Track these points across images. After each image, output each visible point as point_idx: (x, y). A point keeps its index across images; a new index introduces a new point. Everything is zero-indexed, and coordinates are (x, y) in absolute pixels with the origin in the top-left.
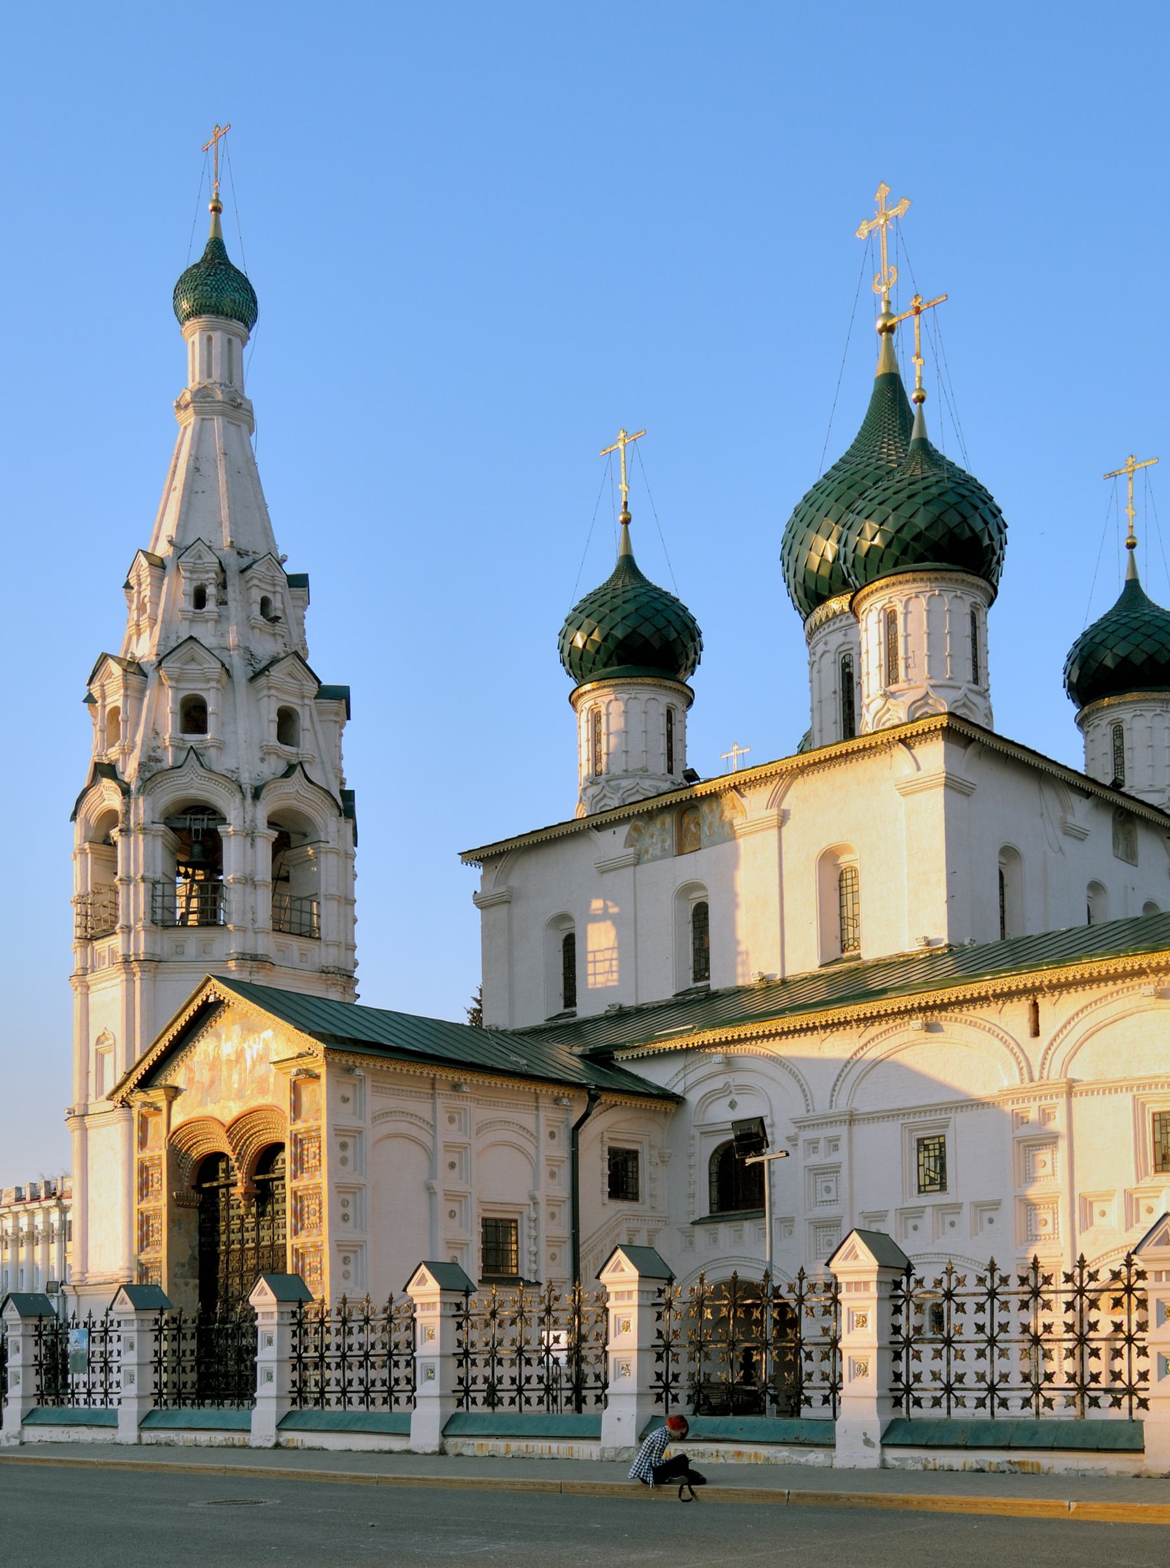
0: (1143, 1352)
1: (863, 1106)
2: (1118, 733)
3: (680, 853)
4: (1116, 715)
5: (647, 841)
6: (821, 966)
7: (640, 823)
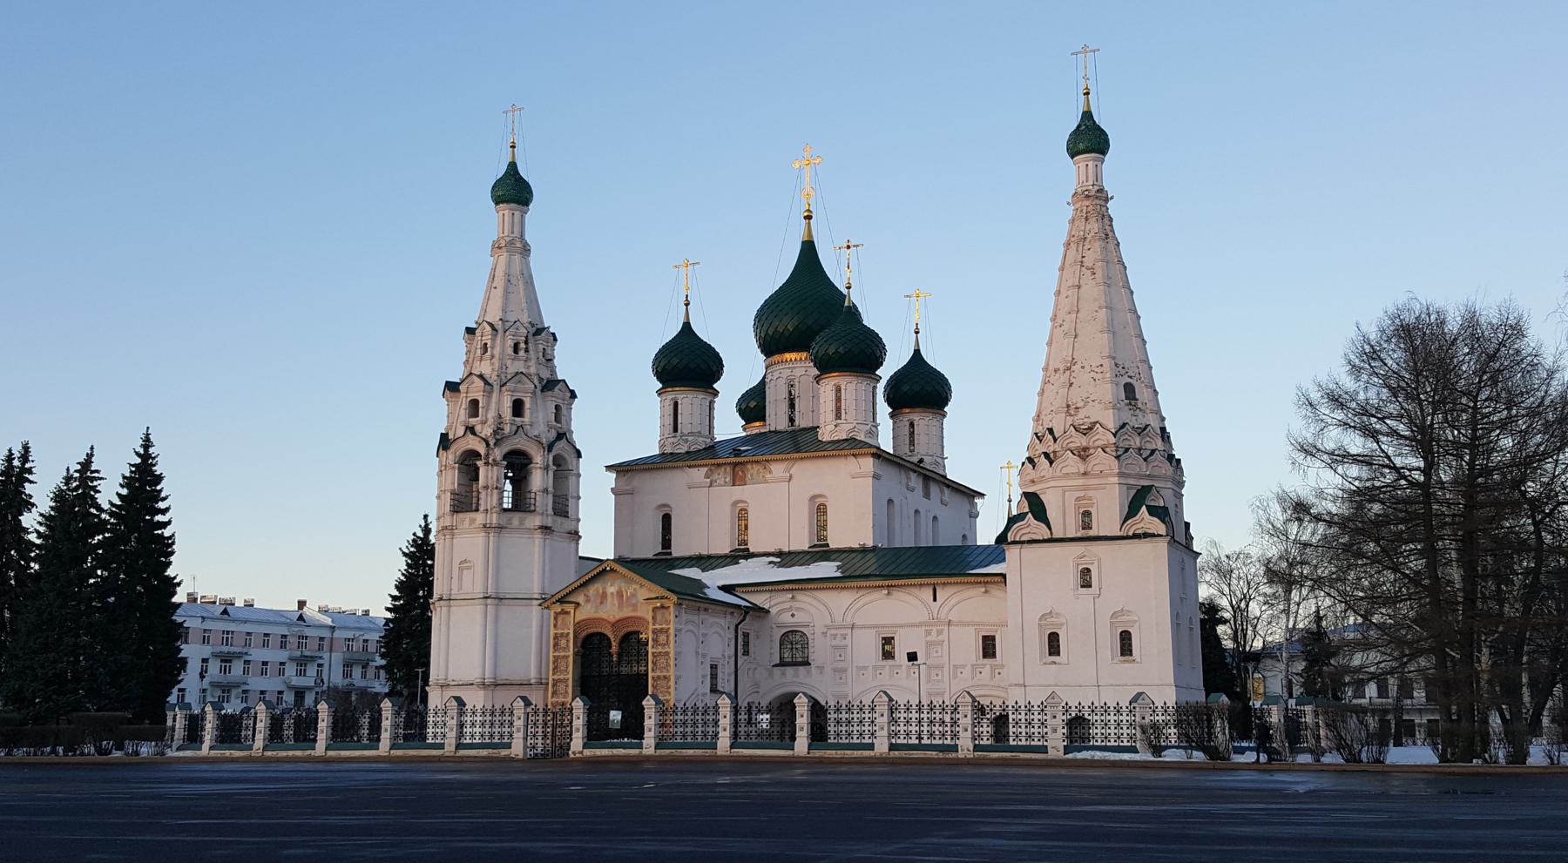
0: (1046, 727)
1: (858, 622)
2: (912, 425)
3: (734, 485)
4: (911, 417)
5: (715, 476)
6: (809, 548)
7: (713, 468)
